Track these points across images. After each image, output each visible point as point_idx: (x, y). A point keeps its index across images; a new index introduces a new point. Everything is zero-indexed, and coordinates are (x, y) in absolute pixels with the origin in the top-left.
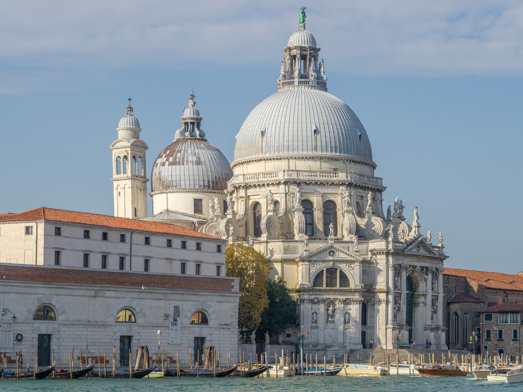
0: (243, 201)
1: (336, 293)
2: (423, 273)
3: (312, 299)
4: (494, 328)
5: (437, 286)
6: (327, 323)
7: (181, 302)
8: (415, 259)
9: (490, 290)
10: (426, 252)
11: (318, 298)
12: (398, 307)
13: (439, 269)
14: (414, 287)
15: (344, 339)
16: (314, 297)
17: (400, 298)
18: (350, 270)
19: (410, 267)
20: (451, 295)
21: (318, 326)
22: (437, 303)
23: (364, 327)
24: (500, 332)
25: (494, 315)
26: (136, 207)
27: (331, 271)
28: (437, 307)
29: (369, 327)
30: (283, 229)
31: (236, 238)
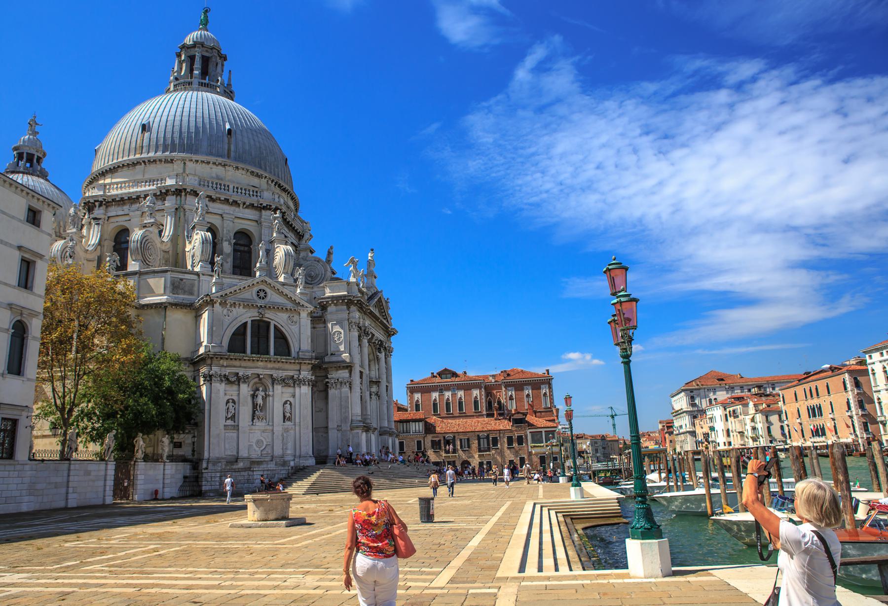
0: (99, 224)
1: (270, 365)
2: (376, 348)
3: (227, 374)
15: (283, 449)
16: (229, 371)
18: (290, 326)
27: (261, 327)
29: (315, 428)
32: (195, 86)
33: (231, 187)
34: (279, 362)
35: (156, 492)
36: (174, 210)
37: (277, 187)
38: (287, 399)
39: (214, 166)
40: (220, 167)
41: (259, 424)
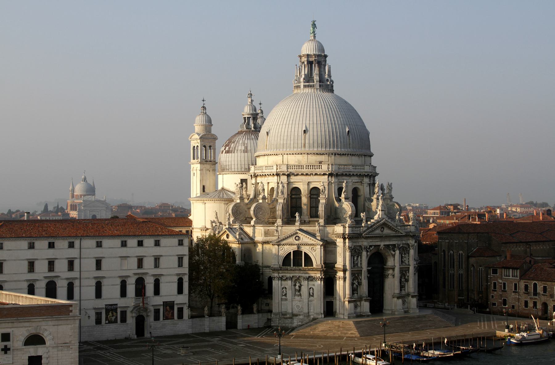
1: (301, 272)
2: (390, 250)
4: (499, 281)
6: (295, 296)
7: (12, 329)
9: (508, 245)
10: (392, 232)
11: (286, 276)
12: (358, 282)
13: (410, 244)
14: (385, 261)
15: (308, 310)
17: (361, 274)
19: (372, 247)
20: (473, 249)
21: (287, 299)
22: (408, 274)
23: (332, 298)
24: (504, 284)
25: (499, 270)
26: (204, 185)
27: (297, 253)
28: (408, 277)
30: (273, 212)
31: (245, 218)
32: (302, 87)
33: (305, 166)
35: (249, 326)
36: (277, 184)
37: (337, 155)
39: (297, 155)
40: (299, 155)
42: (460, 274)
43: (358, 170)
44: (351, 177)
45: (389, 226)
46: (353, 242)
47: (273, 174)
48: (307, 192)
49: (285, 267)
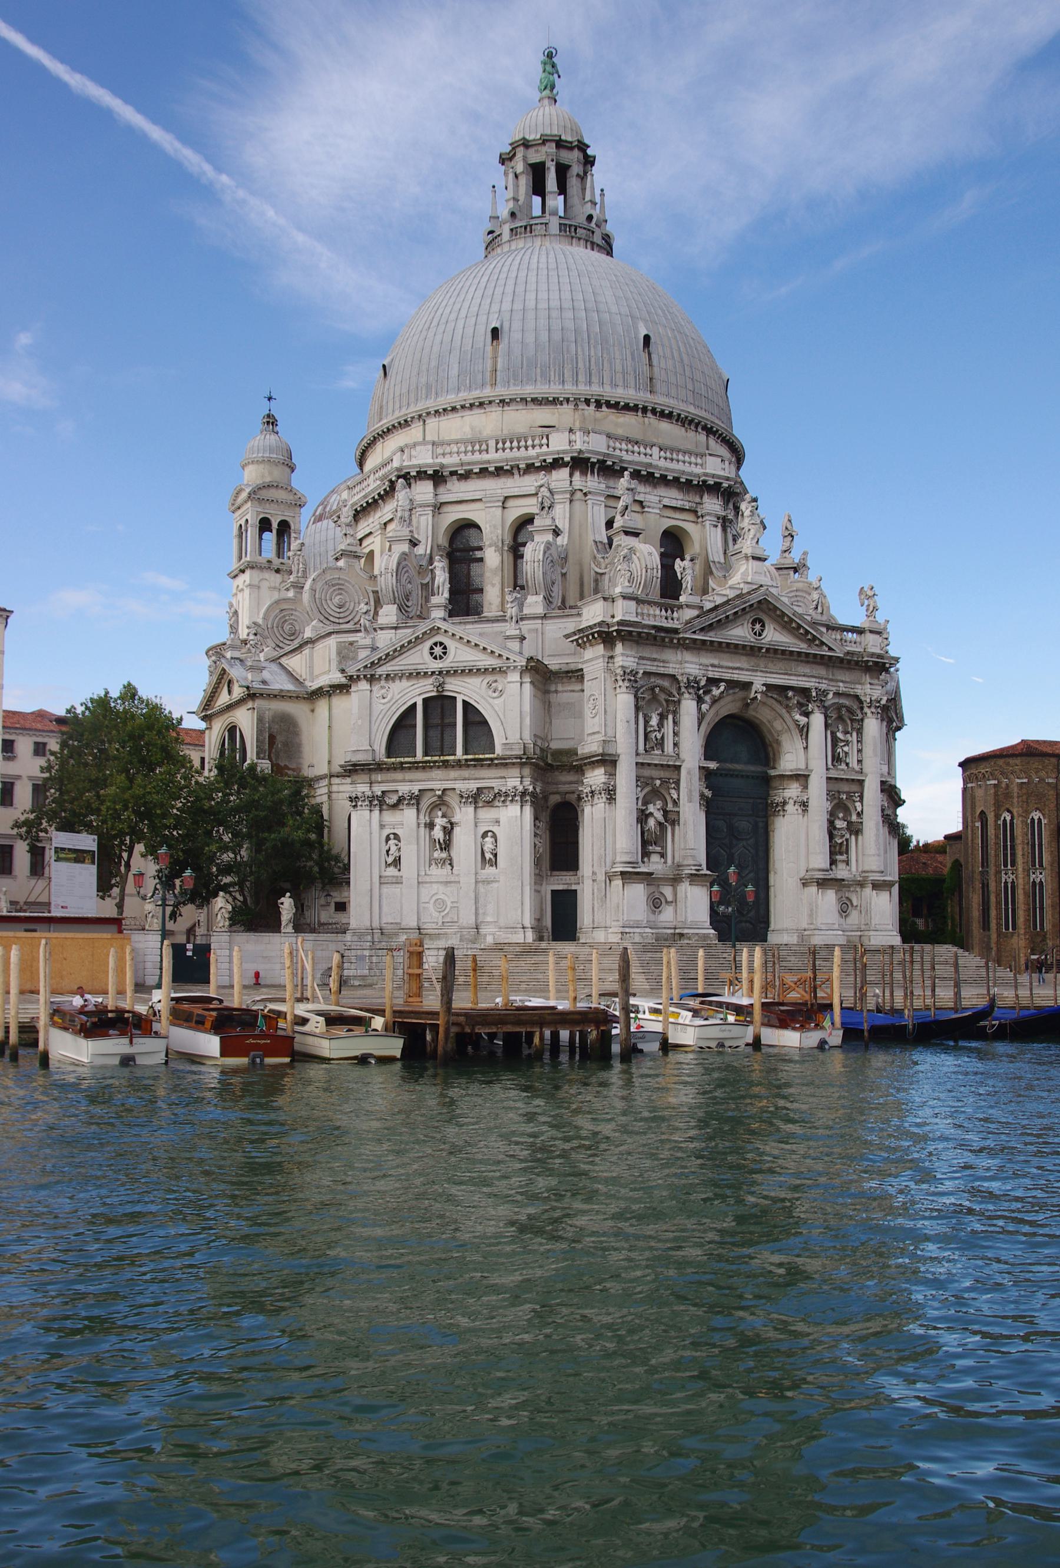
1: (453, 773)
3: (379, 793)
5: (860, 751)
8: (742, 662)
13: (863, 698)
14: (771, 755)
15: (477, 914)
17: (677, 783)
18: (491, 700)
22: (858, 804)
28: (859, 815)
34: (468, 766)
37: (604, 408)
38: (487, 829)
39: (467, 413)
40: (476, 411)
41: (439, 873)
42: (1034, 882)
43: (680, 467)
44: (655, 486)
45: (784, 614)
46: (641, 658)
47: (391, 481)
48: (500, 532)
49: (393, 760)
